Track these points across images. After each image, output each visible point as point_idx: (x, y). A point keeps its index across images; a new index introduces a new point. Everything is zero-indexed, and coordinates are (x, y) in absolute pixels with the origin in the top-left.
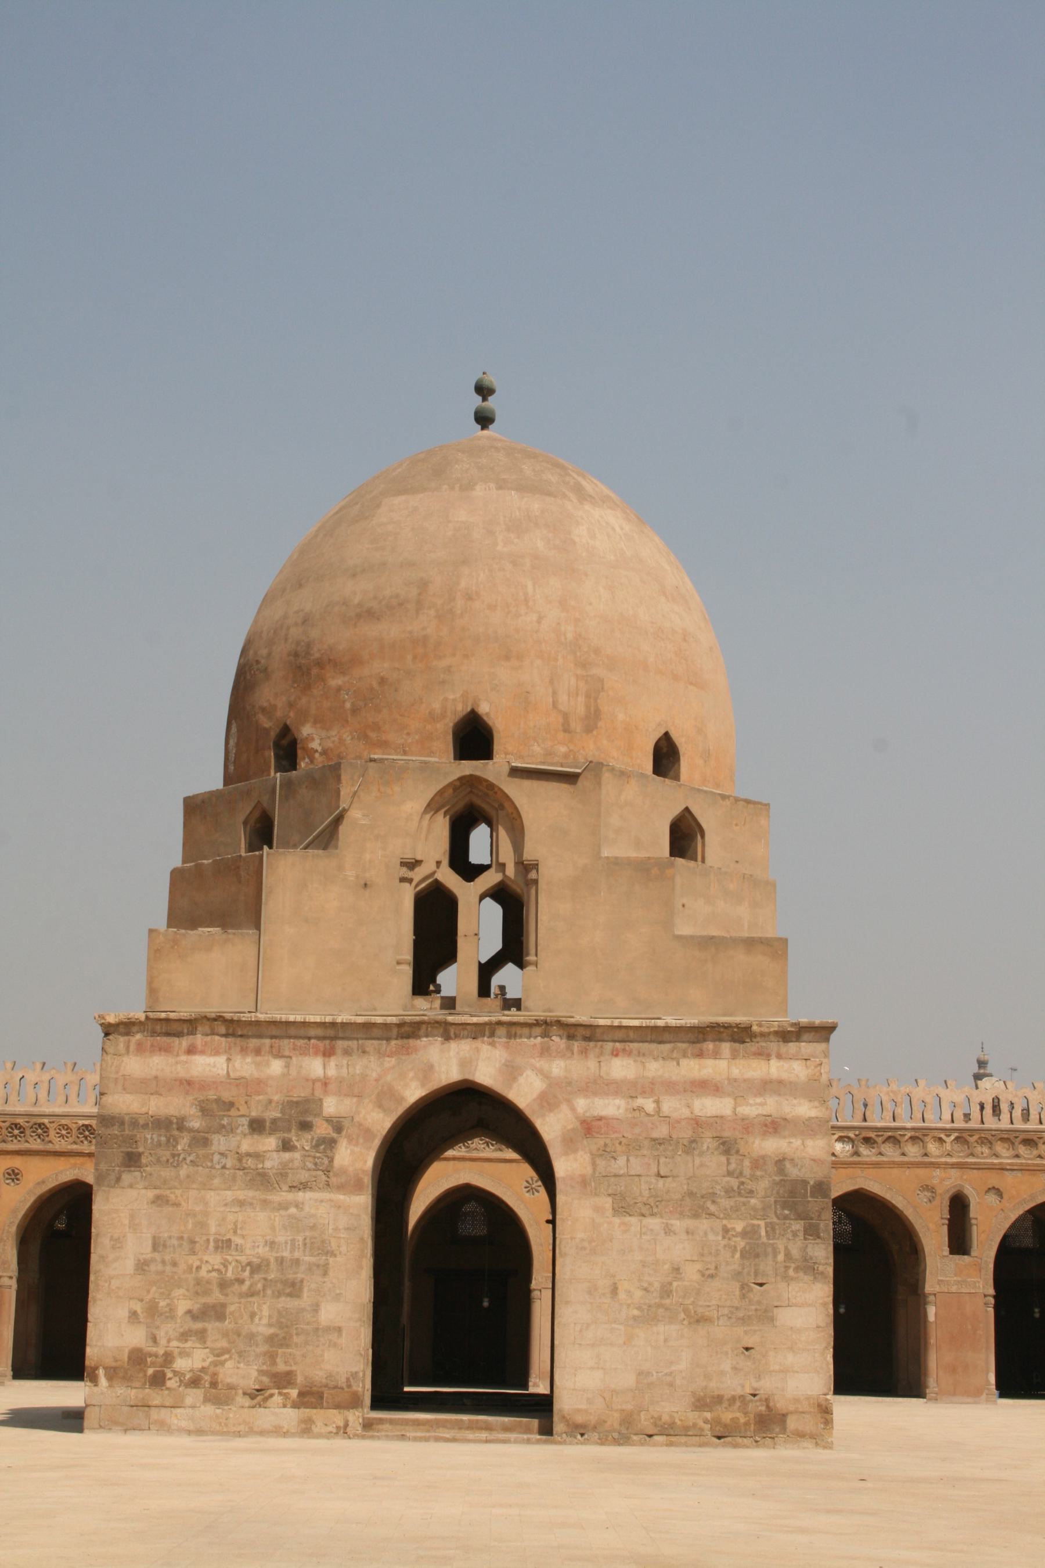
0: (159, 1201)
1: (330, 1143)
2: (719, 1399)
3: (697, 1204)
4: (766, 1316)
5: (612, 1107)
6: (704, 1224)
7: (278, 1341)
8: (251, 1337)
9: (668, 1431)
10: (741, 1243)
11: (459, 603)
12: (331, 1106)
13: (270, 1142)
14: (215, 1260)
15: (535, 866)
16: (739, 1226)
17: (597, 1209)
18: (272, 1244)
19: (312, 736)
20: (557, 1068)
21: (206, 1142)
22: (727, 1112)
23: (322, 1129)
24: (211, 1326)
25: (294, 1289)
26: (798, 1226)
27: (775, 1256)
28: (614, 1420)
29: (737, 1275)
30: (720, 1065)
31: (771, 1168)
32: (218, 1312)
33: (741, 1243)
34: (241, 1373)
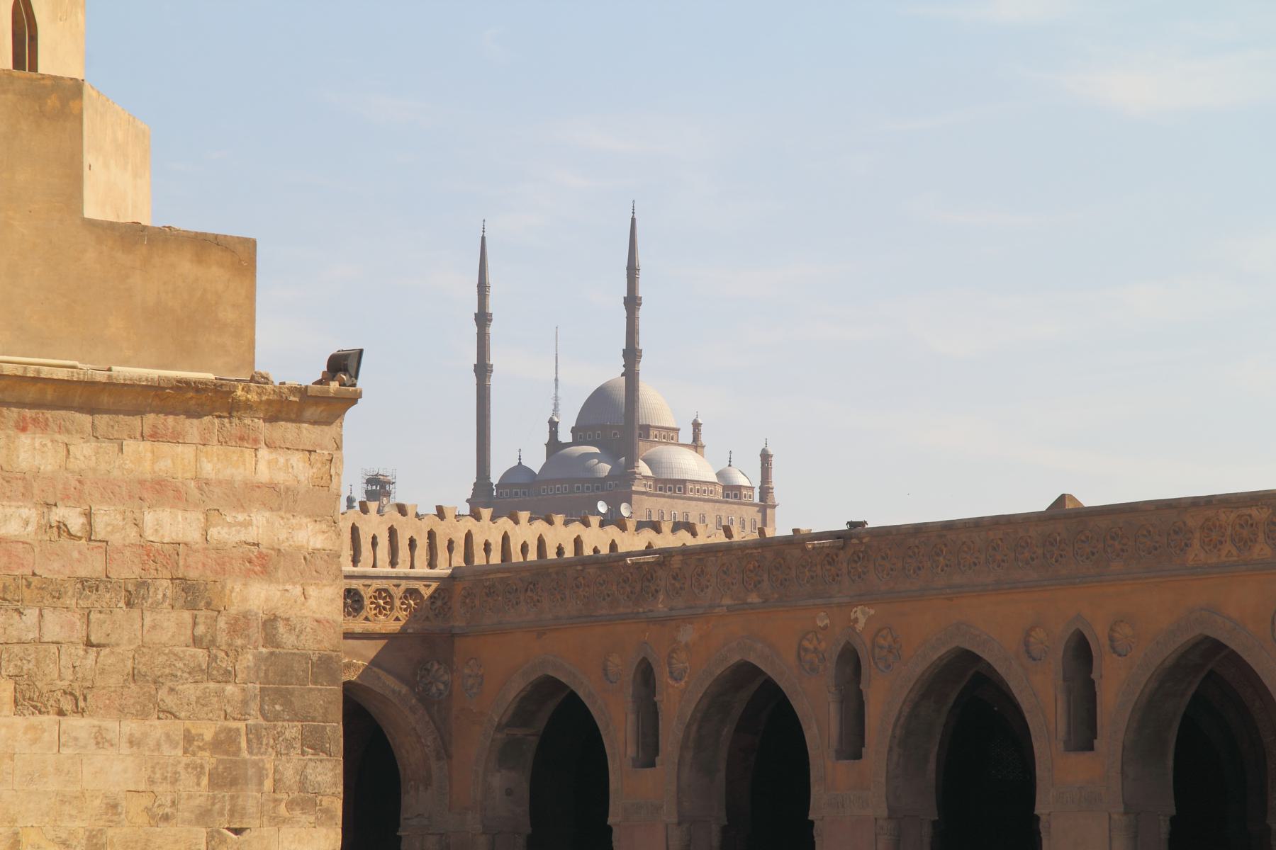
3: (146, 689)
6: (157, 728)
10: (208, 760)
16: (208, 731)
22: (194, 535)
26: (293, 730)
27: (261, 783)
29: (203, 816)
30: (193, 454)
31: (256, 633)
33: (208, 760)
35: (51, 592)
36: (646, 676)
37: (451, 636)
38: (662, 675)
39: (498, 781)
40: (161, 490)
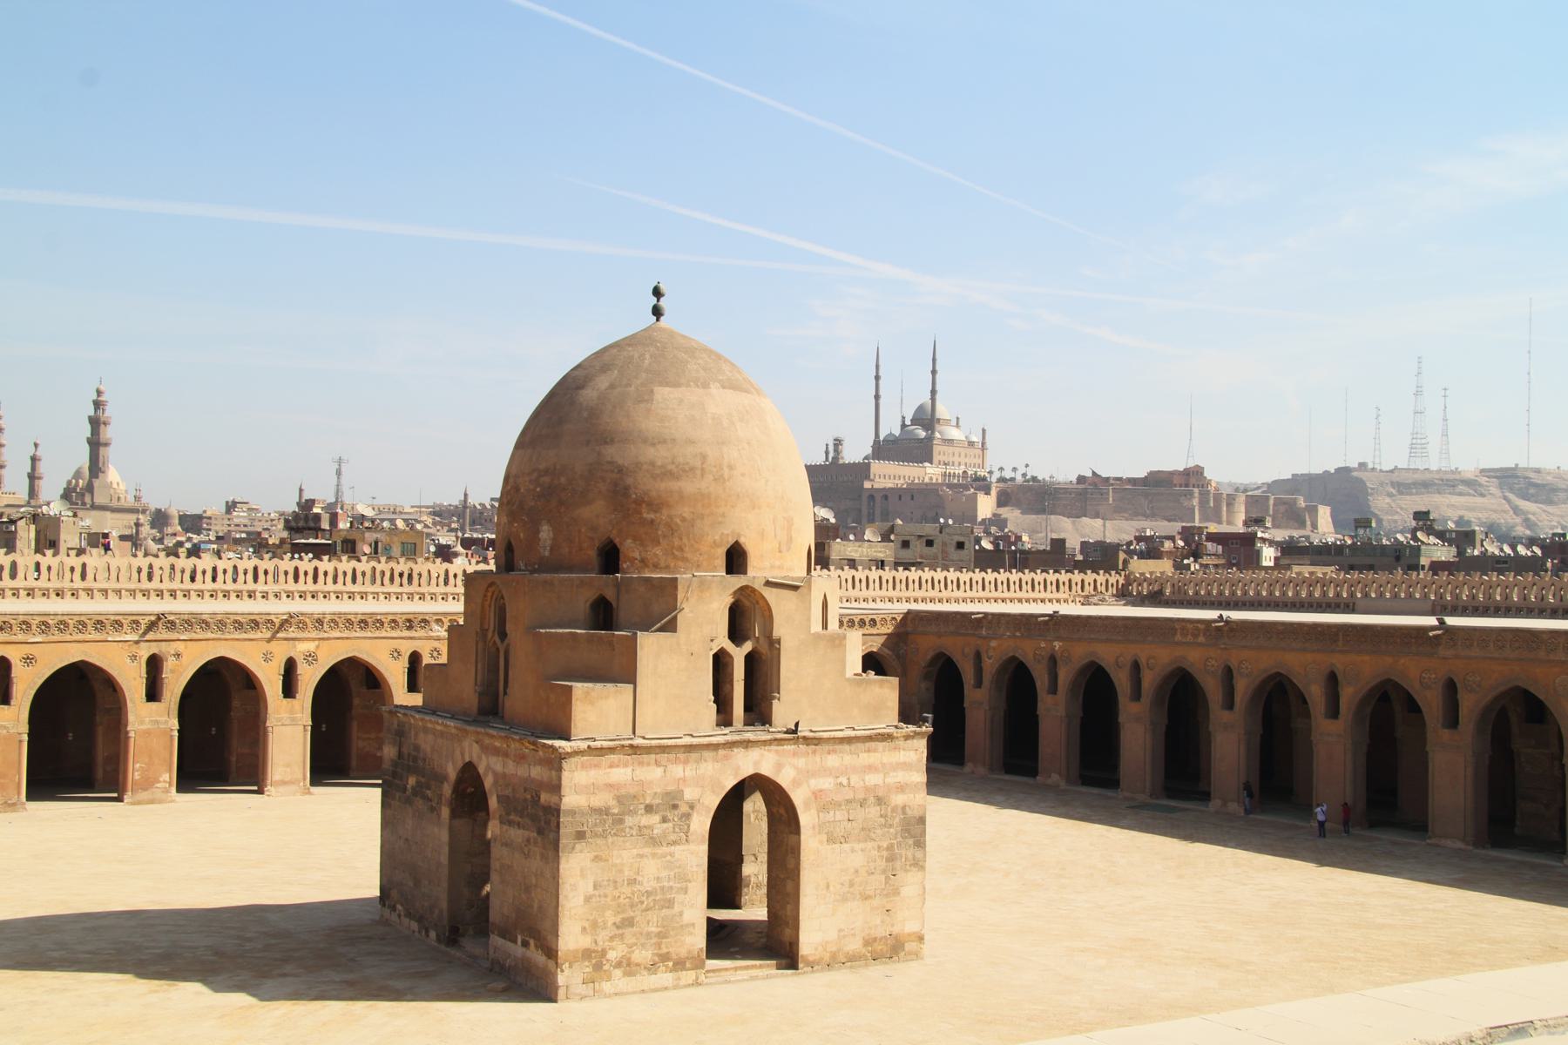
0: (597, 858)
1: (687, 816)
2: (875, 940)
3: (866, 833)
4: (896, 892)
5: (826, 783)
6: (870, 845)
7: (661, 935)
8: (648, 935)
9: (852, 959)
10: (885, 853)
11: (726, 471)
12: (689, 794)
13: (656, 818)
14: (627, 890)
15: (779, 641)
17: (821, 842)
18: (658, 879)
19: (629, 549)
20: (801, 762)
21: (621, 821)
23: (684, 808)
24: (628, 931)
25: (670, 903)
26: (911, 841)
28: (827, 957)
29: (884, 872)
32: (629, 922)
33: (885, 853)
34: (643, 955)
35: (838, 805)
36: (978, 656)
37: (907, 634)
38: (984, 657)
39: (923, 686)
40: (871, 768)
